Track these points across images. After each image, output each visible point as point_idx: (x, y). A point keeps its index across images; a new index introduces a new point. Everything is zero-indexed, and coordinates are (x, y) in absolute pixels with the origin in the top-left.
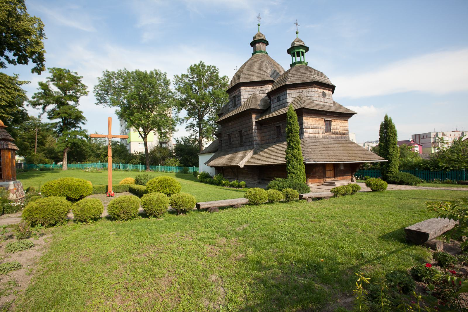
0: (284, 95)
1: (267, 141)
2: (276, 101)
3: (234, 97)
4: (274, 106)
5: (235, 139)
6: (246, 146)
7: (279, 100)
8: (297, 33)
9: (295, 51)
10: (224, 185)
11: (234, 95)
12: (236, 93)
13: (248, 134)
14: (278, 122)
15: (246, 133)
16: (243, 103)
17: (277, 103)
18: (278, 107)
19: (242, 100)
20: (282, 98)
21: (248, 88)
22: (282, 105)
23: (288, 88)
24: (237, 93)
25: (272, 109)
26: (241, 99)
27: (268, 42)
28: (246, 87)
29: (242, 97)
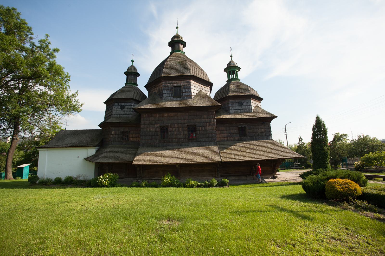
0: (247, 102)
1: (226, 139)
2: (236, 104)
3: (175, 87)
4: (235, 109)
5: (175, 133)
6: (201, 141)
7: (241, 104)
8: (231, 56)
9: (236, 70)
10: (192, 186)
11: (175, 85)
12: (182, 83)
13: (206, 130)
14: (242, 124)
15: (201, 128)
16: (193, 97)
17: (238, 107)
18: (240, 110)
19: (193, 94)
20: (245, 104)
21: (196, 83)
22: (245, 110)
23: (252, 98)
24: (182, 84)
25: (231, 111)
26: (190, 92)
27: (185, 46)
28: (195, 82)
29: (192, 91)
